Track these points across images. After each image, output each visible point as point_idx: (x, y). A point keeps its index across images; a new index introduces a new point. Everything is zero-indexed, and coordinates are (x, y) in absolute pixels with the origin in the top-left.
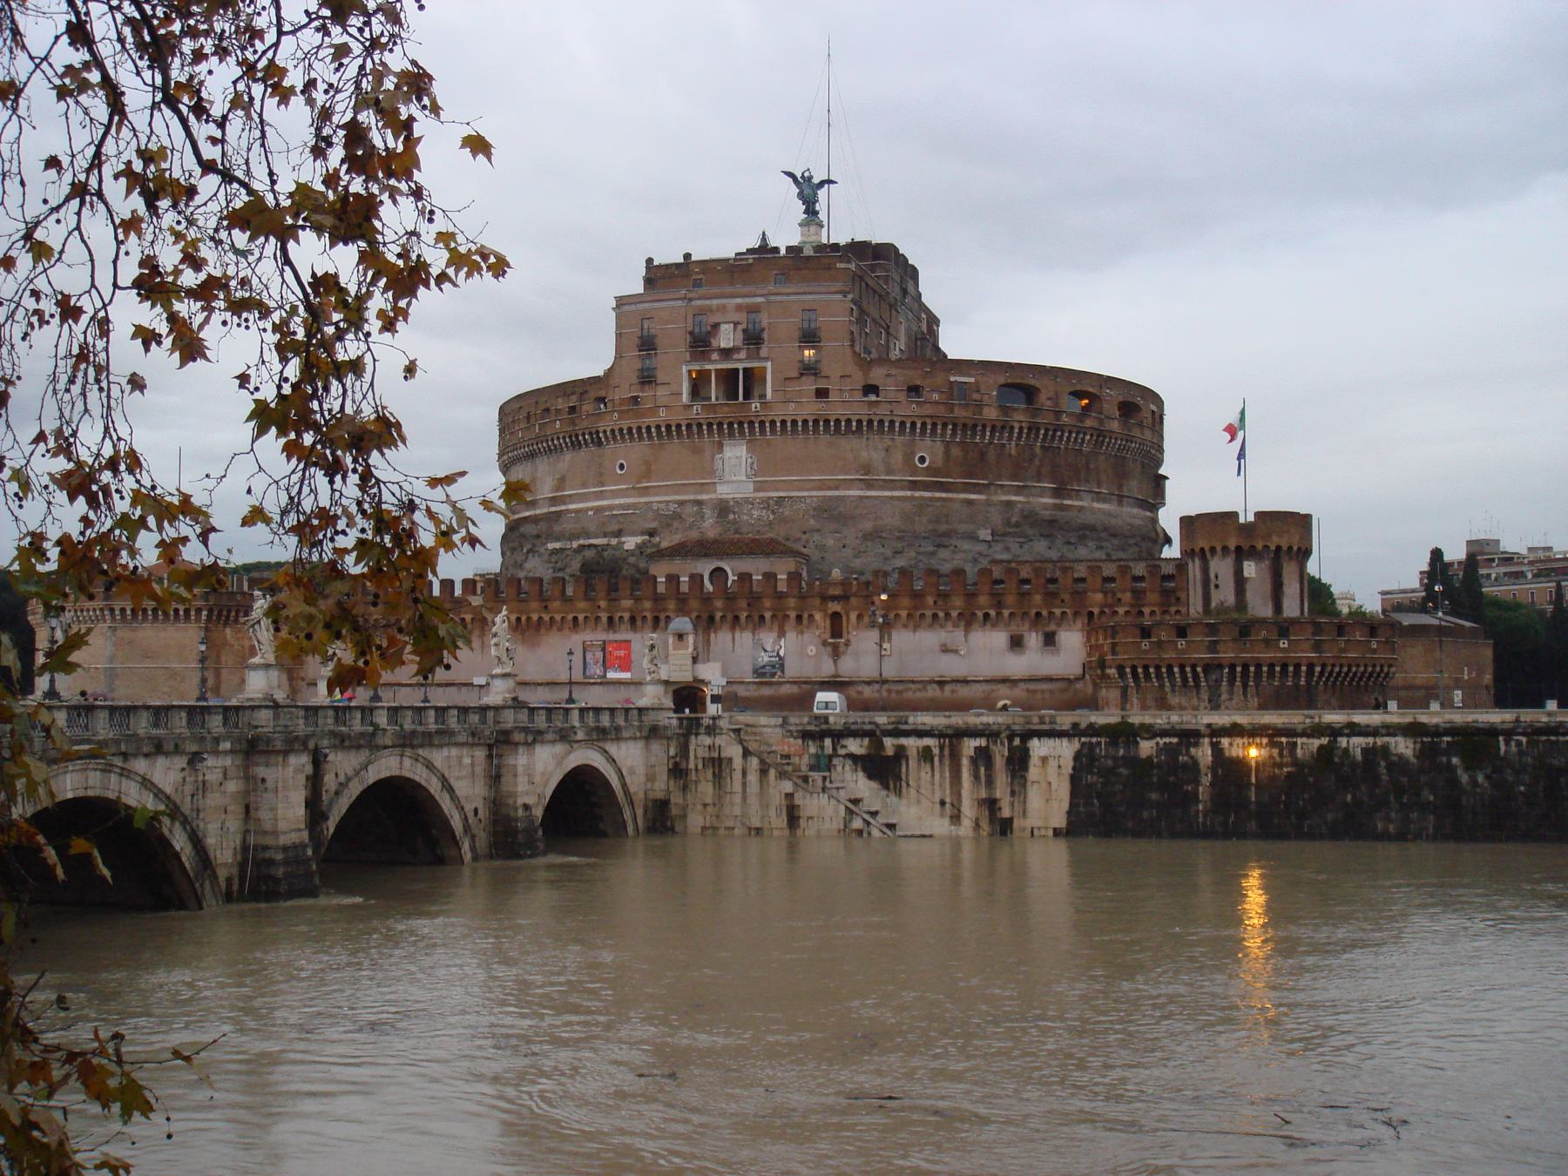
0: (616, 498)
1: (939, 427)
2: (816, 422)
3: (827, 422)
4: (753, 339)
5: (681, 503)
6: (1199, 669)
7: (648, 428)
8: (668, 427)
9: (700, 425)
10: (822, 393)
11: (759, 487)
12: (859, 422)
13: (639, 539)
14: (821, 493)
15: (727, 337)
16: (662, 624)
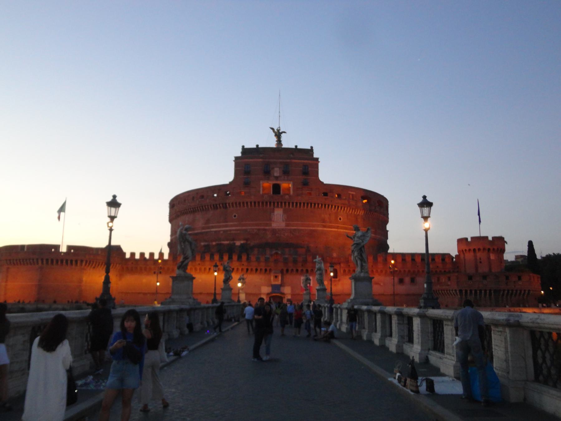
0: (232, 227)
1: (346, 208)
2: (308, 204)
3: (311, 204)
4: (286, 173)
5: (259, 230)
6: (492, 292)
7: (247, 203)
8: (255, 203)
9: (267, 203)
10: (310, 194)
11: (287, 225)
12: (322, 205)
13: (242, 242)
14: (309, 228)
15: (277, 172)
16: (268, 272)
